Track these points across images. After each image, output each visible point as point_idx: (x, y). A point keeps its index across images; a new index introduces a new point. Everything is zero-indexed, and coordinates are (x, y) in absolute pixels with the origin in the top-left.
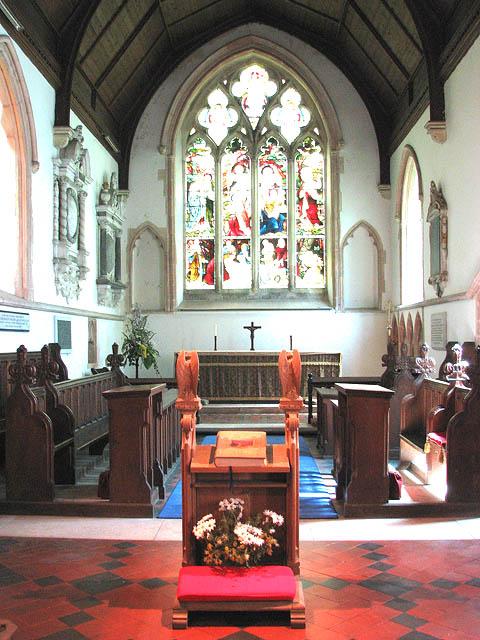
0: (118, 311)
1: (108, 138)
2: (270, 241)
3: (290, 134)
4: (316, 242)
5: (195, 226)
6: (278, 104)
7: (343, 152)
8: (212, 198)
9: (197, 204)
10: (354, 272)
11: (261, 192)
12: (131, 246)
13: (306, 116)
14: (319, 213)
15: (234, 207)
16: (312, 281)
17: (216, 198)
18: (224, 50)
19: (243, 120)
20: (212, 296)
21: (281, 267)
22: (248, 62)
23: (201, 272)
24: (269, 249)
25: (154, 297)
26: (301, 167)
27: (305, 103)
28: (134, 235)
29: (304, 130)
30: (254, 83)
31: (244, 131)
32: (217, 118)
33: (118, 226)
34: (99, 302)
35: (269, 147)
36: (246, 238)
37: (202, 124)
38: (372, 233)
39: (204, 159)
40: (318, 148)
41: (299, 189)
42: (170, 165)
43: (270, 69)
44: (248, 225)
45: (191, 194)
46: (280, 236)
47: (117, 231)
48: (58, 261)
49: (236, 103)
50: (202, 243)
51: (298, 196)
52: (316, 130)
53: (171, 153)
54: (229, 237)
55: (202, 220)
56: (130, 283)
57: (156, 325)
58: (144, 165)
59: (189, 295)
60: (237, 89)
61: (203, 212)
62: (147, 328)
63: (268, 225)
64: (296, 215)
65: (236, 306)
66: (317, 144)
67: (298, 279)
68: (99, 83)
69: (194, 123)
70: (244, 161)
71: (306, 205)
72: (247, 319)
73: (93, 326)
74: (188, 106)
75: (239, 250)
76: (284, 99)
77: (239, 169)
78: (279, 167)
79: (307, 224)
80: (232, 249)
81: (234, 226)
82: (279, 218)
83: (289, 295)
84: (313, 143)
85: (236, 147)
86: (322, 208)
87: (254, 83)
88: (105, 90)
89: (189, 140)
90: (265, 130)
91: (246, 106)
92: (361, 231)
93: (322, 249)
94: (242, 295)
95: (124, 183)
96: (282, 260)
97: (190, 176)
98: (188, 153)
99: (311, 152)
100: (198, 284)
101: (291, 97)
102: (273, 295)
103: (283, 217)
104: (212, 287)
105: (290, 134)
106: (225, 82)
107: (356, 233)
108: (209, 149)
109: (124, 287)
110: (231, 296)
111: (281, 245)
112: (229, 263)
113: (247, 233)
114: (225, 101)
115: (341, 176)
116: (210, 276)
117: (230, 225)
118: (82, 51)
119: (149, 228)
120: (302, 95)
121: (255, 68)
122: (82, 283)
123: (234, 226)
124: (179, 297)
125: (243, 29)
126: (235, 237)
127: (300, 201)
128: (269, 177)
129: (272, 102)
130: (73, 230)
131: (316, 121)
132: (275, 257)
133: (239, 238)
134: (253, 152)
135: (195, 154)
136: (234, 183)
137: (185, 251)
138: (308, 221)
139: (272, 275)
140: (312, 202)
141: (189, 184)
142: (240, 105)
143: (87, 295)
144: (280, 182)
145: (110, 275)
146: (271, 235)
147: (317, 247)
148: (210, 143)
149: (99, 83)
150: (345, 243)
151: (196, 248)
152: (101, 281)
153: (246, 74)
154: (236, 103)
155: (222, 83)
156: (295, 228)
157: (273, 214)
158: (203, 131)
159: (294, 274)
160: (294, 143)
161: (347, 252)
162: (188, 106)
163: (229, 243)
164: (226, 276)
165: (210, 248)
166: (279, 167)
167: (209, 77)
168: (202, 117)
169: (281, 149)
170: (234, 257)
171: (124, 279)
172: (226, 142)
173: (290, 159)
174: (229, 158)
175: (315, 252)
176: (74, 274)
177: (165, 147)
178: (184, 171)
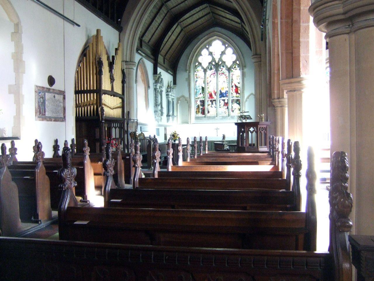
2: (223, 100)
3: (229, 64)
4: (238, 100)
8: (204, 86)
11: (219, 84)
12: (177, 103)
14: (238, 90)
15: (211, 89)
17: (205, 86)
18: (206, 37)
21: (226, 109)
22: (215, 40)
23: (200, 111)
24: (222, 102)
26: (233, 75)
30: (217, 46)
31: (214, 63)
32: (204, 58)
35: (222, 69)
36: (215, 99)
40: (238, 68)
41: (232, 82)
42: (189, 76)
44: (215, 95)
45: (197, 85)
46: (226, 98)
47: (173, 99)
49: (211, 54)
50: (201, 101)
51: (232, 84)
53: (190, 72)
54: (209, 99)
55: (200, 94)
58: (181, 76)
60: (211, 49)
63: (222, 95)
64: (231, 91)
68: (165, 56)
69: (197, 61)
70: (214, 73)
75: (212, 104)
76: (226, 52)
79: (235, 94)
80: (210, 103)
81: (211, 96)
82: (226, 92)
83: (229, 118)
85: (211, 69)
87: (217, 46)
89: (196, 67)
90: (220, 63)
93: (240, 102)
95: (175, 83)
96: (226, 106)
97: (196, 79)
98: (195, 71)
99: (236, 69)
101: (230, 51)
103: (227, 92)
104: (204, 116)
105: (229, 64)
106: (207, 47)
107: (250, 97)
108: (203, 70)
109: (175, 116)
111: (226, 101)
114: (207, 53)
117: (210, 95)
118: (161, 49)
119: (183, 96)
120: (233, 51)
122: (162, 117)
123: (211, 96)
126: (211, 99)
127: (232, 87)
128: (222, 79)
129: (223, 53)
131: (237, 60)
133: (213, 99)
134: (217, 70)
136: (211, 81)
138: (235, 93)
140: (236, 87)
141: (196, 82)
142: (212, 54)
144: (226, 81)
146: (223, 98)
147: (238, 102)
148: (203, 68)
149: (165, 56)
150: (246, 101)
151: (199, 103)
154: (211, 54)
155: (206, 47)
156: (231, 96)
157: (223, 91)
158: (200, 64)
159: (230, 111)
160: (230, 67)
163: (209, 101)
164: (208, 112)
166: (226, 75)
167: (202, 45)
168: (200, 59)
169: (226, 69)
170: (211, 106)
172: (208, 68)
173: (229, 73)
174: (209, 72)
175: (237, 104)
176: (160, 115)
177: (187, 70)
178: (194, 78)
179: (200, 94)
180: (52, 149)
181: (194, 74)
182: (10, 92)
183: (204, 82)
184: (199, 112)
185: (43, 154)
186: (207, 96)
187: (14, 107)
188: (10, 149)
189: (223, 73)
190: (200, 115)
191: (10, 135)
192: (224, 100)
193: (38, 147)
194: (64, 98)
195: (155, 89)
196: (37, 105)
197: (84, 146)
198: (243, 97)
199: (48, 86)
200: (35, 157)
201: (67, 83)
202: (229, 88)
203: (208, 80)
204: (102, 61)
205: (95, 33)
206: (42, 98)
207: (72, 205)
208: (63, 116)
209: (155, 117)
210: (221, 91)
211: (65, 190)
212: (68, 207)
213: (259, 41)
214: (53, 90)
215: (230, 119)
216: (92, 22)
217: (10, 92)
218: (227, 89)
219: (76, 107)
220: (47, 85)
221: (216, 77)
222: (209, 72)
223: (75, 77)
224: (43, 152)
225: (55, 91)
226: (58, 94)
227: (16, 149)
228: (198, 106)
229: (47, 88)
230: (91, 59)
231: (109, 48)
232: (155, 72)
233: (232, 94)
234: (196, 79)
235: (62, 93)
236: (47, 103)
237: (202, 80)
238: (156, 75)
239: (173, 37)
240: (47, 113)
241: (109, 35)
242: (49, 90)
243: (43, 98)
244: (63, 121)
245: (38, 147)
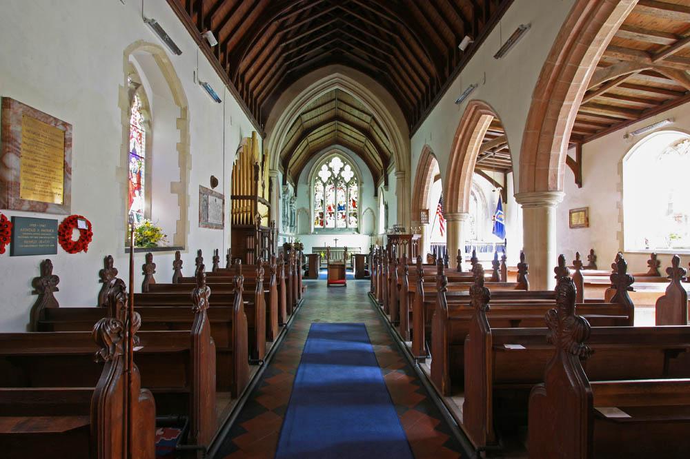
3: (347, 180)
4: (355, 213)
5: (318, 208)
6: (344, 170)
7: (363, 186)
10: (365, 226)
11: (338, 198)
12: (298, 214)
13: (352, 174)
15: (330, 202)
16: (353, 225)
20: (324, 230)
22: (334, 157)
24: (340, 215)
28: (298, 210)
29: (352, 178)
30: (336, 163)
32: (324, 174)
38: (372, 211)
39: (320, 187)
42: (310, 189)
43: (341, 158)
46: (344, 212)
48: (284, 222)
49: (330, 169)
50: (320, 213)
58: (302, 188)
59: (316, 229)
60: (331, 165)
63: (340, 208)
64: (349, 205)
69: (317, 176)
71: (352, 202)
72: (335, 237)
75: (331, 216)
77: (331, 190)
79: (352, 208)
85: (330, 184)
87: (336, 163)
89: (316, 181)
92: (369, 210)
95: (296, 196)
100: (319, 226)
101: (348, 167)
102: (341, 229)
105: (347, 180)
110: (328, 229)
111: (344, 214)
112: (328, 220)
113: (333, 210)
116: (322, 223)
119: (303, 209)
123: (330, 208)
124: (312, 231)
125: (333, 146)
128: (341, 193)
129: (342, 169)
131: (355, 176)
134: (336, 185)
137: (315, 215)
139: (341, 223)
140: (354, 201)
146: (341, 211)
147: (355, 215)
148: (322, 182)
151: (318, 215)
154: (330, 169)
157: (342, 205)
158: (320, 178)
161: (364, 217)
165: (322, 215)
168: (320, 174)
173: (347, 187)
174: (328, 187)
177: (308, 183)
183: (324, 196)
186: (327, 208)
189: (342, 188)
190: (319, 226)
195: (284, 200)
198: (360, 211)
203: (329, 193)
218: (345, 203)
222: (328, 187)
224: (154, 264)
228: (317, 218)
232: (284, 183)
234: (315, 192)
239: (300, 151)
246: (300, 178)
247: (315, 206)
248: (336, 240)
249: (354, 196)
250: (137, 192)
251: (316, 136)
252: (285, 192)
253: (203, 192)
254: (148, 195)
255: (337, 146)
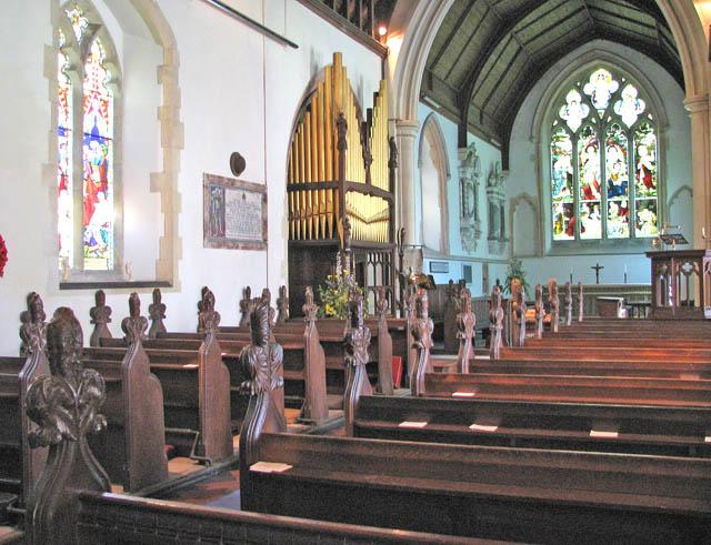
0: (505, 256)
1: (493, 141)
2: (615, 202)
4: (651, 202)
7: (670, 134)
8: (571, 172)
9: (560, 176)
12: (512, 210)
19: (593, 111)
22: (596, 68)
23: (564, 227)
24: (614, 208)
25: (530, 246)
26: (638, 145)
27: (639, 96)
30: (601, 84)
31: (594, 120)
32: (574, 113)
33: (502, 198)
34: (490, 252)
37: (562, 116)
39: (565, 144)
41: (637, 161)
44: (598, 191)
46: (624, 200)
47: (501, 201)
49: (587, 100)
50: (565, 205)
52: (650, 116)
55: (564, 189)
56: (512, 237)
57: (527, 266)
58: (519, 147)
59: (557, 244)
60: (588, 90)
61: (565, 184)
62: (522, 270)
64: (635, 181)
65: (590, 251)
66: (650, 127)
67: (637, 230)
70: (596, 143)
71: (642, 175)
73: (485, 268)
74: (551, 105)
75: (592, 211)
77: (591, 149)
78: (621, 146)
79: (643, 189)
83: (630, 242)
84: (648, 126)
85: (588, 133)
86: (655, 176)
87: (601, 84)
88: (490, 108)
89: (553, 130)
90: (609, 119)
91: (595, 102)
94: (593, 243)
95: (506, 166)
100: (562, 236)
101: (630, 91)
102: (618, 242)
104: (573, 238)
109: (508, 240)
111: (624, 205)
112: (584, 219)
115: (668, 153)
116: (571, 229)
119: (524, 196)
121: (601, 71)
123: (588, 192)
124: (548, 246)
125: (589, 45)
128: (614, 154)
129: (616, 97)
130: (471, 209)
132: (619, 215)
134: (601, 136)
135: (558, 140)
138: (644, 187)
139: (618, 228)
143: (482, 249)
144: (622, 159)
145: (497, 232)
146: (616, 198)
147: (651, 205)
148: (569, 131)
151: (560, 210)
152: (491, 238)
153: (594, 77)
157: (617, 183)
158: (563, 123)
162: (551, 105)
163: (584, 205)
164: (583, 230)
165: (571, 209)
171: (507, 234)
173: (630, 140)
179: (564, 189)
180: (239, 308)
181: (549, 146)
182: (153, 189)
183: (573, 163)
184: (561, 229)
185: (217, 317)
186: (582, 193)
187: (161, 217)
188: (151, 307)
189: (616, 142)
191: (152, 278)
192: (619, 203)
193: (206, 302)
194: (265, 200)
195: (462, 181)
196: (207, 214)
197: (303, 300)
198: (663, 194)
199: (231, 176)
200: (202, 324)
201: (270, 168)
202: (630, 174)
203: (584, 157)
204: (345, 121)
205: (329, 61)
206: (219, 199)
207: (272, 430)
208: (261, 239)
209: (463, 241)
210: (610, 182)
211: (256, 395)
212: (262, 435)
213: (702, 61)
214: (242, 181)
215: (632, 245)
216: (324, 38)
217: (153, 189)
218: (626, 178)
219: (290, 220)
220: (227, 173)
221: (598, 151)
222: (583, 142)
223: (288, 156)
225: (246, 185)
226: (251, 191)
227: (164, 307)
228: (560, 218)
229: (229, 179)
230: (320, 118)
231: (360, 90)
232: (462, 143)
233: (637, 187)
235: (261, 190)
236: (227, 210)
237: (568, 159)
238: (463, 149)
240: (227, 231)
241: (360, 65)
242: (232, 184)
243: (221, 199)
244: (261, 249)
245: (206, 302)
246: (515, 128)
247: (552, 190)
248: (597, 268)
249: (647, 160)
250: (101, 195)
251: (537, 28)
252: (468, 160)
253: (213, 185)
254: (119, 196)
255: (599, 43)
